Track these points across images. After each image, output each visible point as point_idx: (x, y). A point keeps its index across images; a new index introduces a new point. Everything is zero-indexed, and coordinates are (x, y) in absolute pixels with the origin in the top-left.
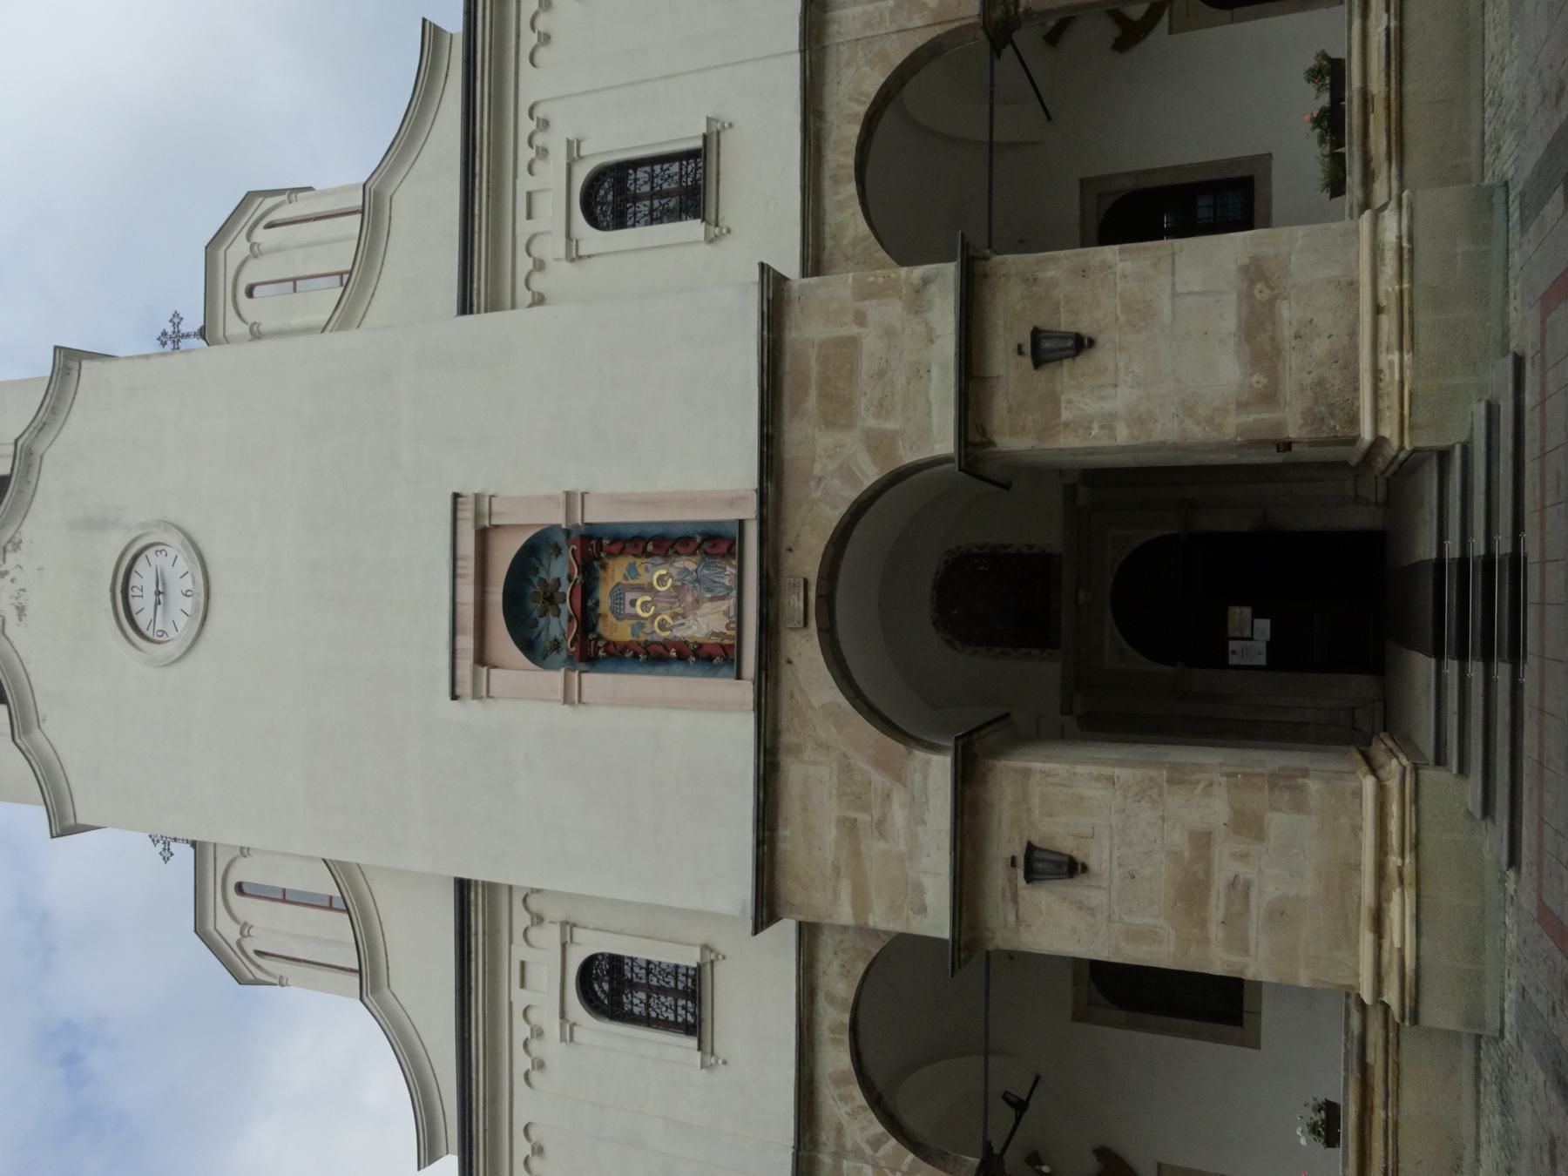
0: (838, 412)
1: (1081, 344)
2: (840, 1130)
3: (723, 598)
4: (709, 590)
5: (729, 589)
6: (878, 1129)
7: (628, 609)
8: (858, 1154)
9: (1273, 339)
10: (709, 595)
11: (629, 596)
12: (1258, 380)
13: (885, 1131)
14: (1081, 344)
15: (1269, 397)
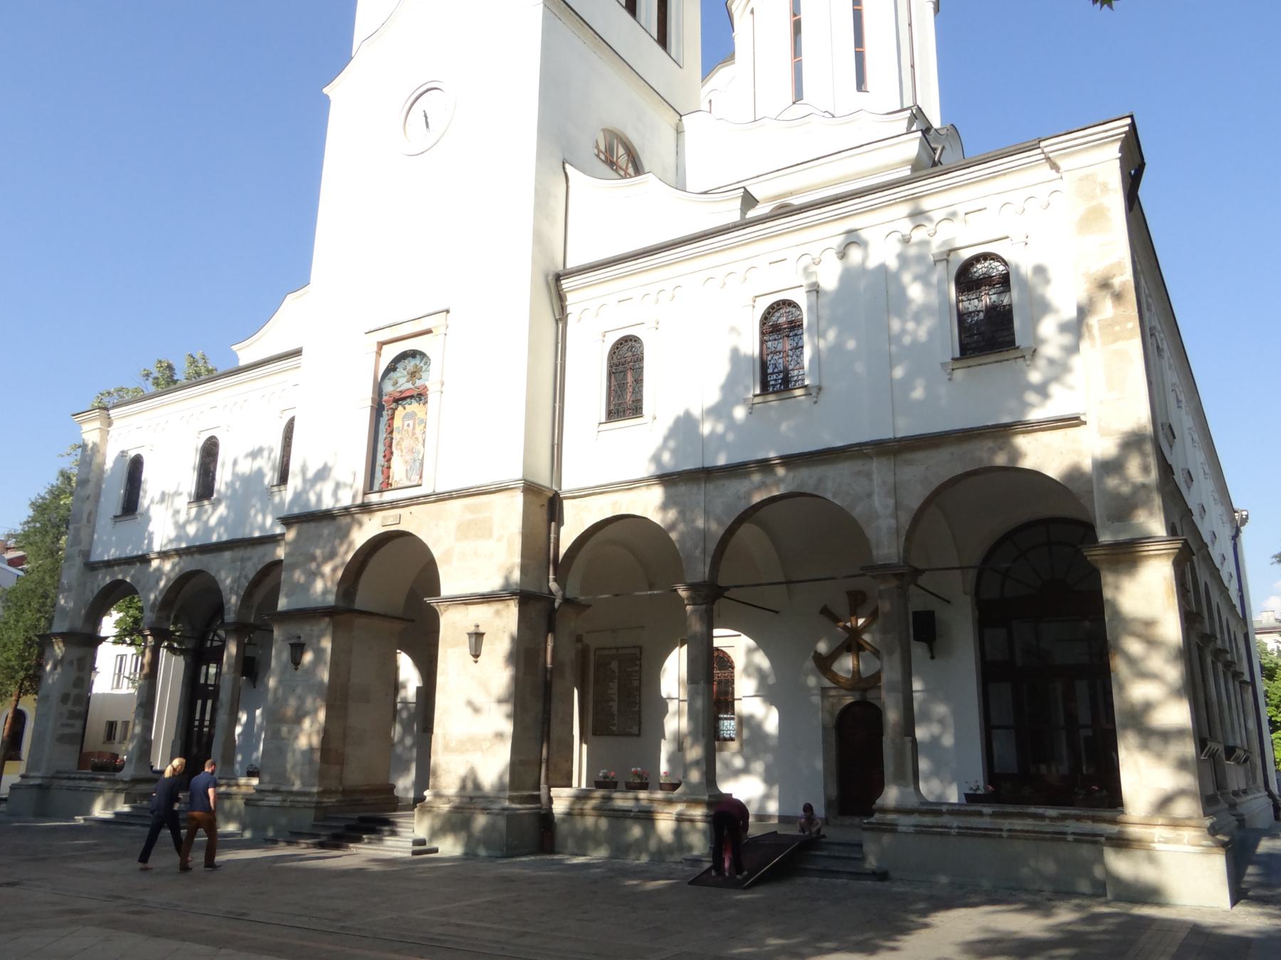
0: (468, 530)
1: (476, 655)
2: (249, 559)
3: (407, 476)
4: (411, 467)
5: (410, 480)
6: (251, 576)
7: (406, 423)
8: (243, 569)
9: (468, 750)
10: (408, 469)
11: (411, 422)
12: (453, 744)
13: (251, 579)
14: (476, 655)
15: (446, 748)
